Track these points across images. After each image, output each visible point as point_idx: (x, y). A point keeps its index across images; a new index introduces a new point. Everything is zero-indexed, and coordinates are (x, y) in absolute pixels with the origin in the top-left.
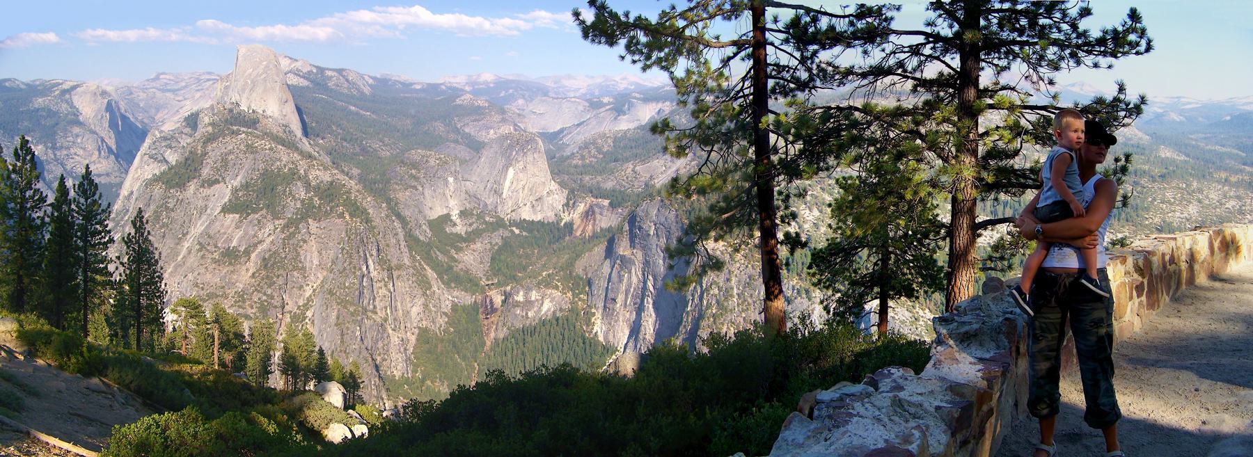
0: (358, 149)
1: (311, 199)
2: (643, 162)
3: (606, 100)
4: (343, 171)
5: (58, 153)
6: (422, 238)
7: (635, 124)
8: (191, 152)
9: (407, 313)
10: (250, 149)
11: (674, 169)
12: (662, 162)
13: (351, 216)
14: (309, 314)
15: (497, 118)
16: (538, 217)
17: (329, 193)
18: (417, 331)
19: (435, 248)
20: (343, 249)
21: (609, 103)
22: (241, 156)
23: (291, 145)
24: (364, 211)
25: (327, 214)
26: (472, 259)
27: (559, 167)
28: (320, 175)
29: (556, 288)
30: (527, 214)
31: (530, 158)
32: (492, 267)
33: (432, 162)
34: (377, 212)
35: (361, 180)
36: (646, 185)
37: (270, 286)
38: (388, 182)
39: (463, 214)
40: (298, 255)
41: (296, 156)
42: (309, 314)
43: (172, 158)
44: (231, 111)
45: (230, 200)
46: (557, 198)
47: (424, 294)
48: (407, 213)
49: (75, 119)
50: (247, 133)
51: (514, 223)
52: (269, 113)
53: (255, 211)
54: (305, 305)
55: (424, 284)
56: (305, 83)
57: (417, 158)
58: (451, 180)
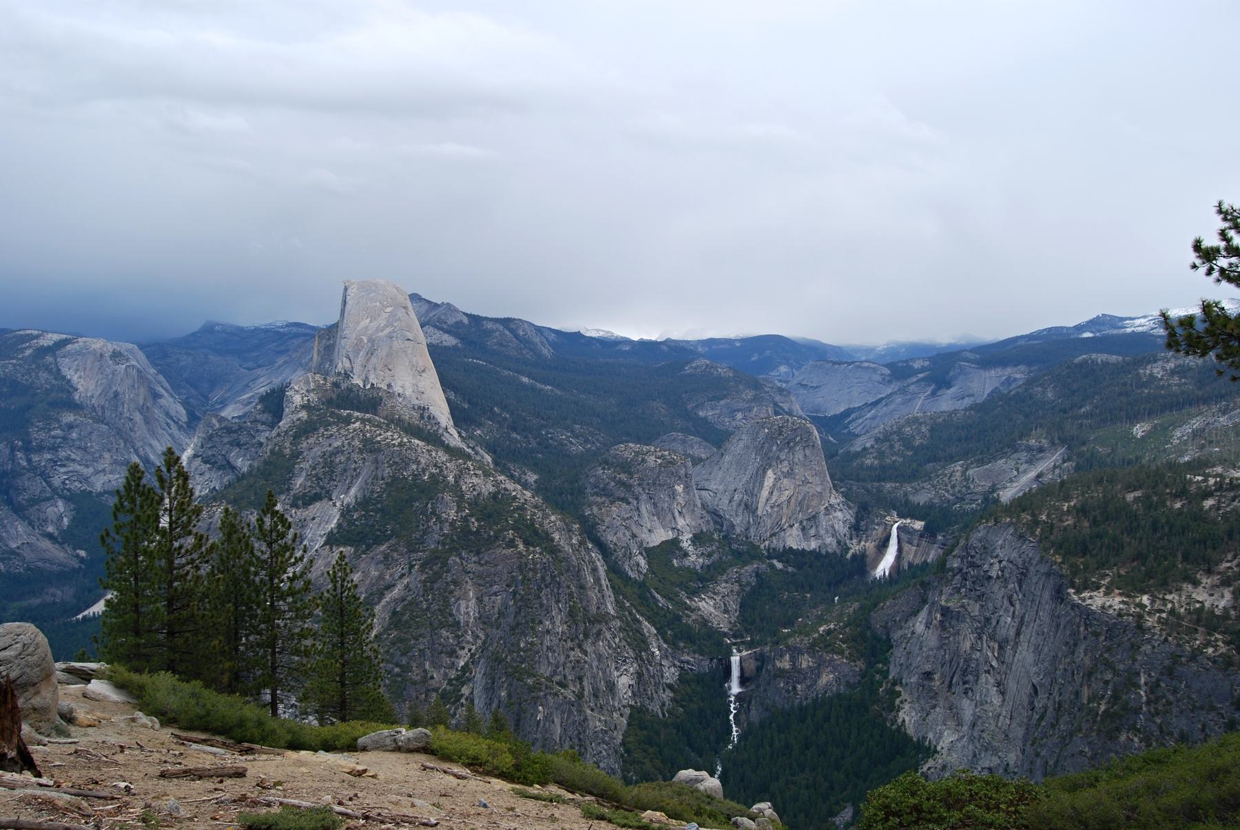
0: (534, 444)
1: (465, 519)
2: (981, 462)
3: (917, 365)
4: (511, 477)
5: (35, 458)
6: (632, 575)
7: (968, 402)
8: (272, 452)
9: (611, 687)
10: (370, 447)
11: (1033, 474)
12: (1012, 463)
13: (527, 543)
14: (465, 690)
15: (749, 394)
16: (813, 545)
17: (494, 509)
18: (628, 711)
19: (654, 594)
20: (515, 593)
21: (922, 370)
22: (355, 456)
23: (434, 439)
24: (548, 538)
25: (491, 542)
26: (710, 608)
27: (844, 471)
28: (479, 484)
29: (841, 653)
30: (793, 540)
31: (799, 456)
32: (743, 618)
33: (651, 460)
34: (565, 539)
35: (539, 489)
36: (986, 500)
37: (403, 654)
38: (581, 491)
39: (698, 539)
40: (447, 604)
41: (442, 456)
42: (465, 690)
43: (242, 463)
44: (336, 385)
45: (339, 526)
46: (841, 519)
47: (638, 657)
48: (610, 538)
49: (65, 399)
50: (363, 421)
51: (773, 554)
52: (397, 389)
53: (378, 541)
54: (457, 679)
55: (640, 644)
56: (449, 340)
57: (629, 455)
58: (679, 488)
